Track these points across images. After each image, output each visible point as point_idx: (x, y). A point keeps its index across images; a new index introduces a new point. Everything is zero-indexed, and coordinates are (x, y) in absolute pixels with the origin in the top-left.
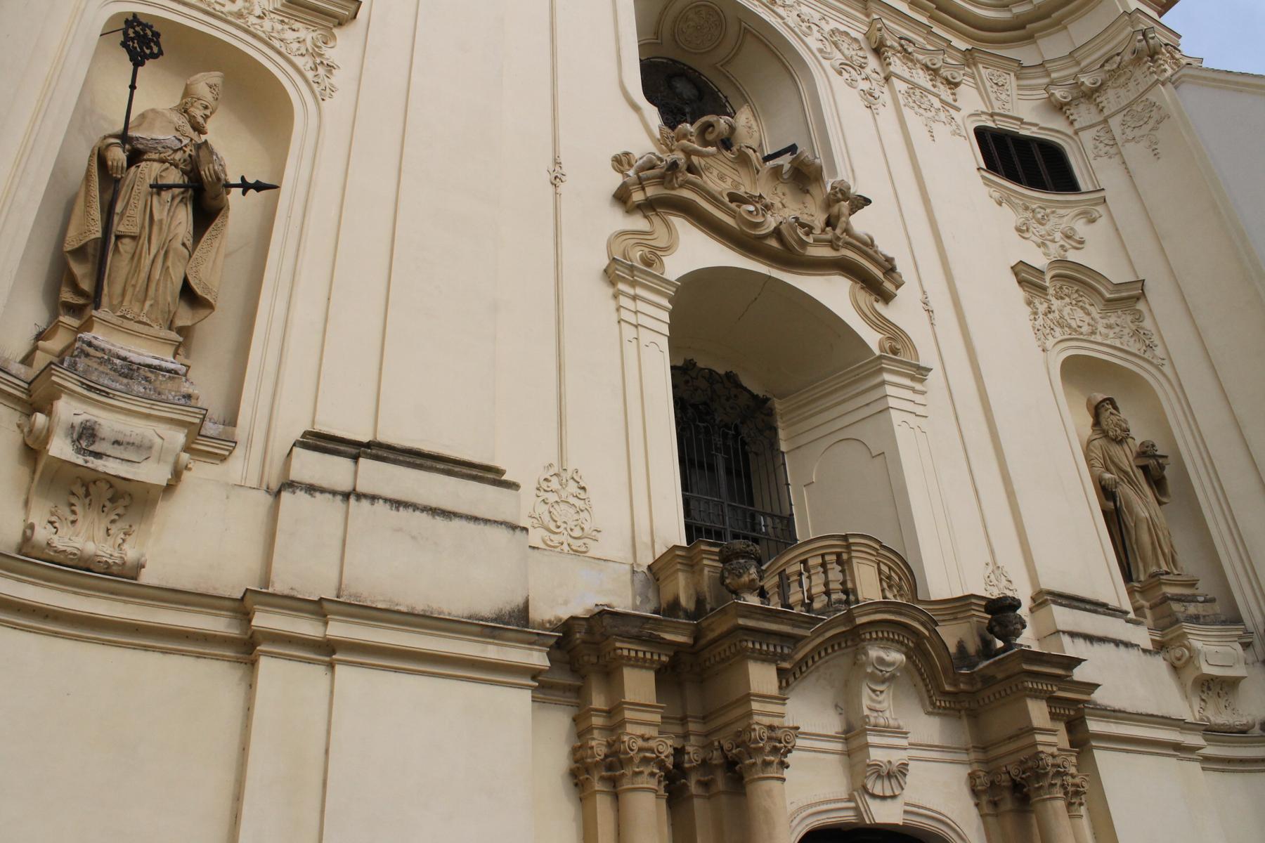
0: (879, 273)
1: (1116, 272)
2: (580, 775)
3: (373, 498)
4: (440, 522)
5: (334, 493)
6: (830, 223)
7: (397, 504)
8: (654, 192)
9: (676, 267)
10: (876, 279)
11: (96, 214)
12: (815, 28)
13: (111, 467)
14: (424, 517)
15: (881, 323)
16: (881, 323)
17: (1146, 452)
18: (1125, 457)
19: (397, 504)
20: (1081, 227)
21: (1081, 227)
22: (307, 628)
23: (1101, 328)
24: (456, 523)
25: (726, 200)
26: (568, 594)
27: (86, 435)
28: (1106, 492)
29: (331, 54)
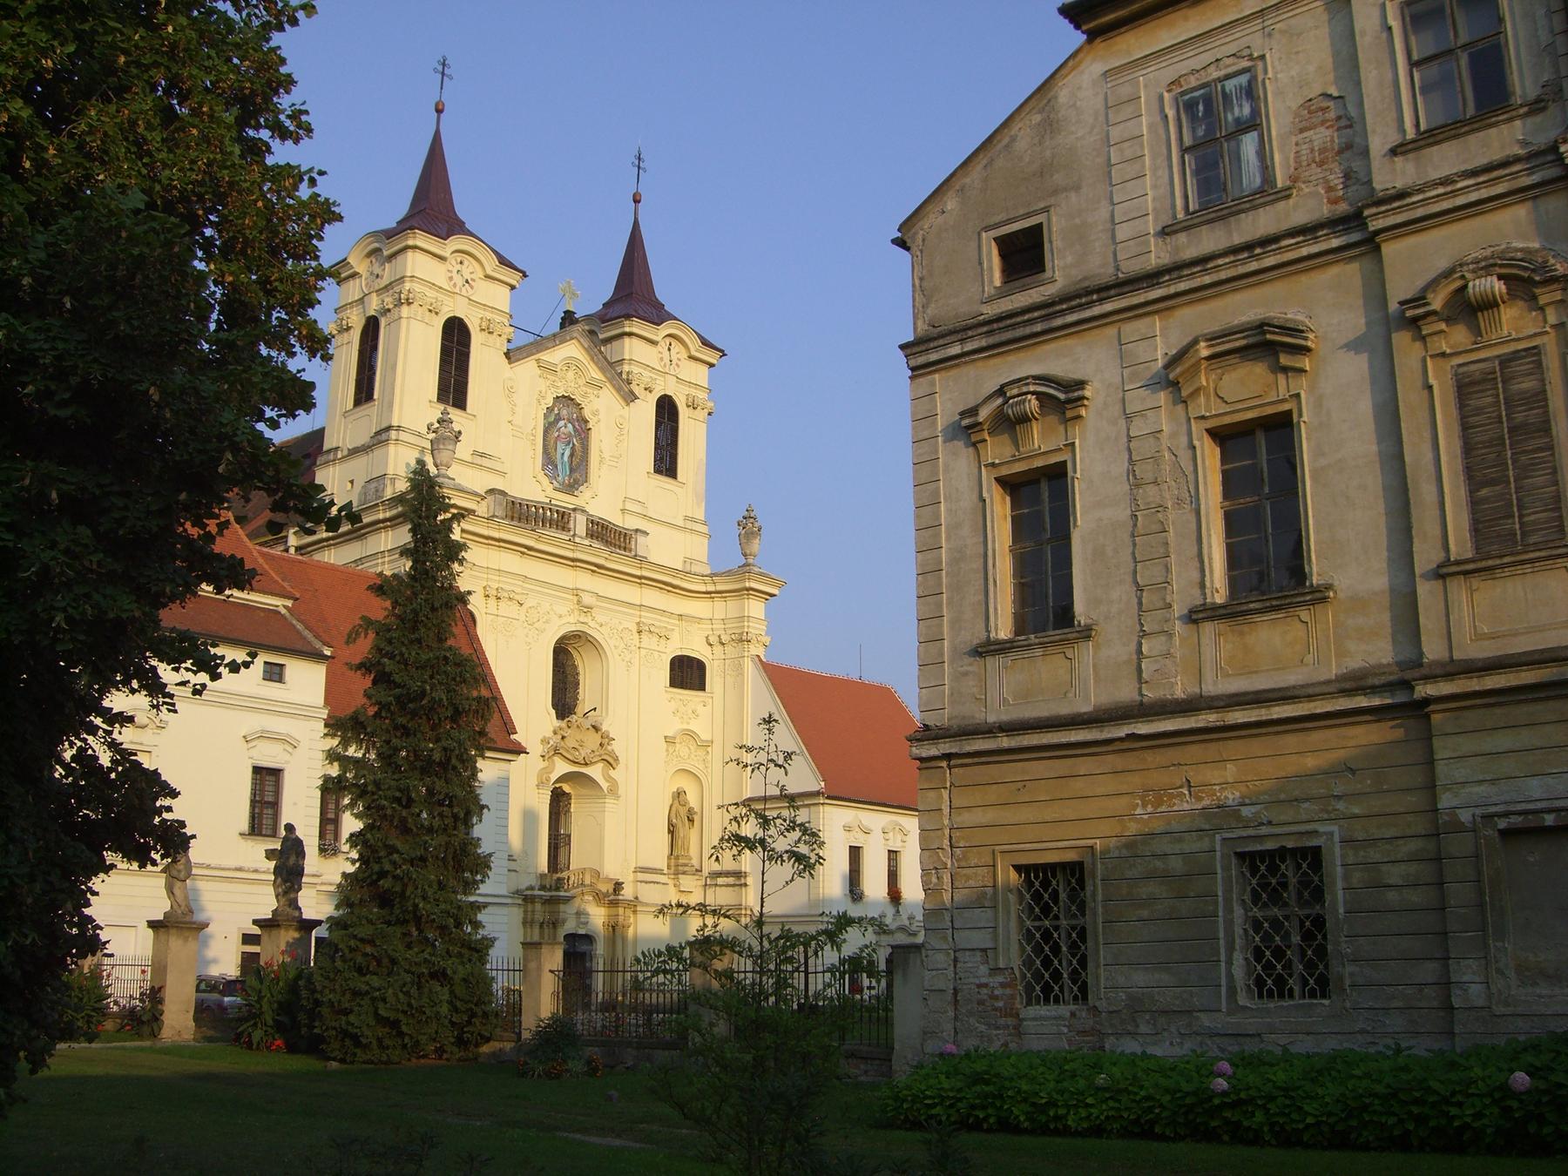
1: (705, 736)
2: (525, 923)
10: (610, 762)
15: (609, 779)
16: (609, 779)
17: (690, 811)
18: (683, 812)
20: (700, 709)
21: (700, 709)
28: (670, 824)
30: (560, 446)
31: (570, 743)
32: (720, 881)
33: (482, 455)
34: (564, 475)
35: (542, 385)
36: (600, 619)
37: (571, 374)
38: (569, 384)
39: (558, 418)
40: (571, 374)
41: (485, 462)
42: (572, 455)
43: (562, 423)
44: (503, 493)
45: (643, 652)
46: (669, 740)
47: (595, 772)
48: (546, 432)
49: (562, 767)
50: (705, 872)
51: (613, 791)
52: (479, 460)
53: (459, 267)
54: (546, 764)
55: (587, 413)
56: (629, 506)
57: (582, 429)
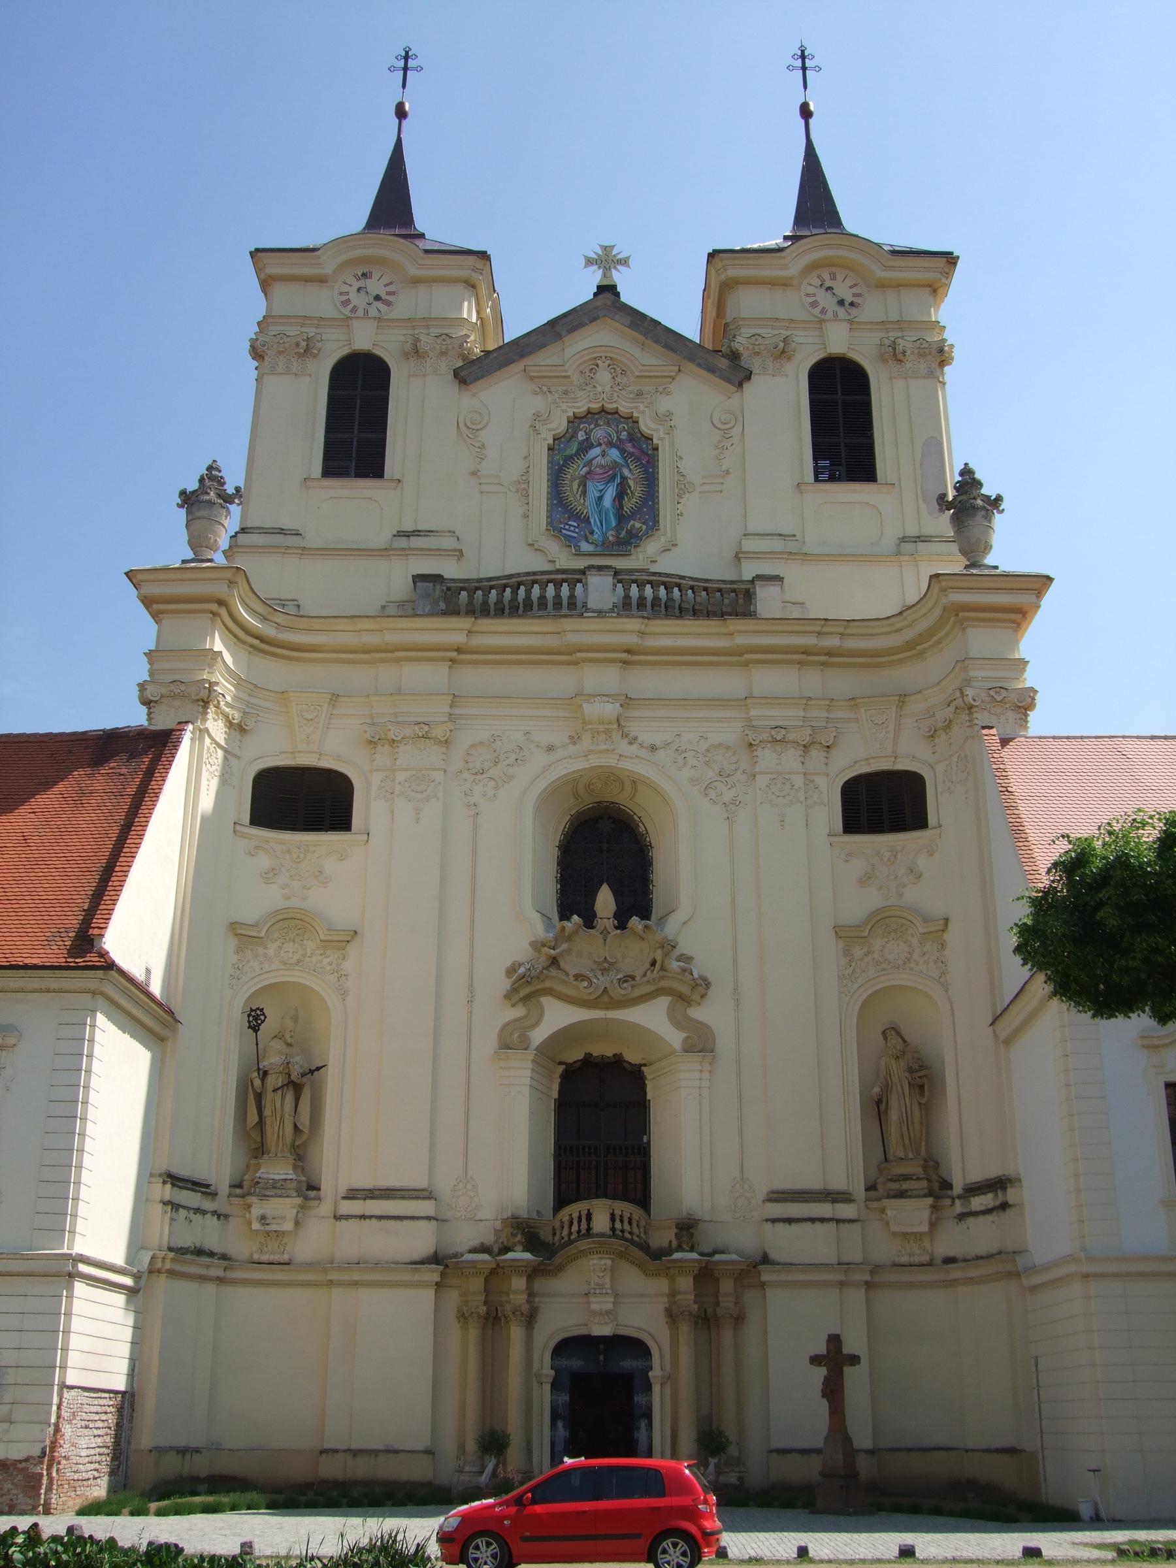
0: (685, 990)
3: (371, 1217)
4: (398, 1223)
5: (356, 1217)
6: (653, 963)
7: (380, 1218)
8: (527, 986)
9: (539, 1035)
11: (255, 1111)
12: (690, 754)
13: (274, 1227)
14: (391, 1222)
18: (899, 1070)
19: (380, 1218)
20: (923, 862)
22: (346, 1277)
23: (916, 956)
24: (406, 1222)
25: (572, 978)
26: (465, 1237)
27: (263, 1218)
29: (347, 965)
30: (593, 489)
31: (572, 965)
32: (977, 1203)
33: (407, 535)
34: (603, 528)
35: (538, 403)
36: (647, 737)
37: (604, 376)
38: (606, 390)
39: (586, 446)
40: (604, 376)
41: (416, 542)
42: (620, 496)
43: (595, 452)
44: (437, 578)
45: (762, 781)
46: (849, 936)
47: (652, 1017)
48: (557, 475)
49: (557, 1016)
50: (958, 1189)
51: (701, 1043)
52: (403, 543)
53: (361, 283)
54: (519, 1012)
55: (647, 425)
56: (749, 545)
57: (642, 452)
